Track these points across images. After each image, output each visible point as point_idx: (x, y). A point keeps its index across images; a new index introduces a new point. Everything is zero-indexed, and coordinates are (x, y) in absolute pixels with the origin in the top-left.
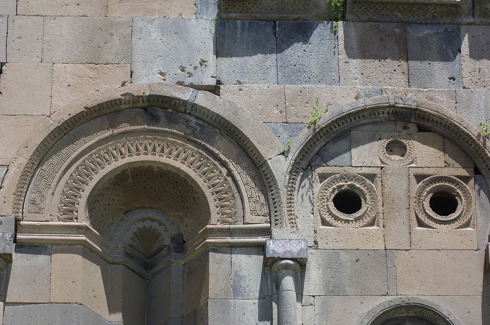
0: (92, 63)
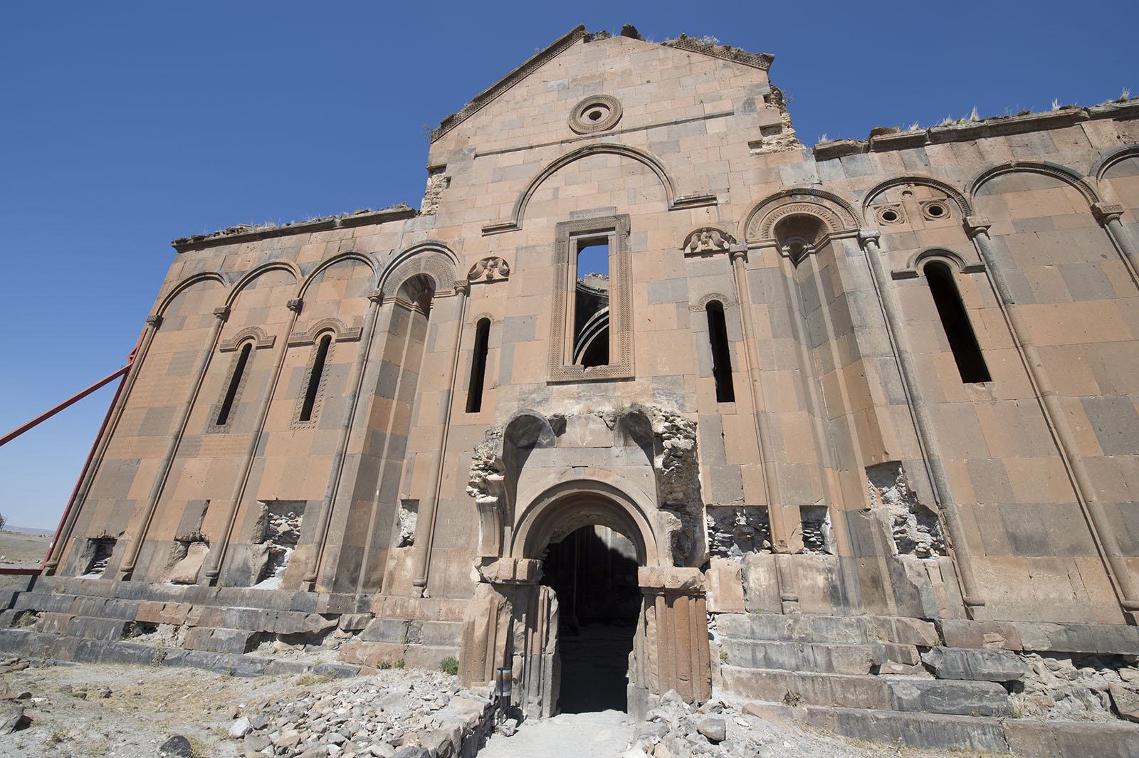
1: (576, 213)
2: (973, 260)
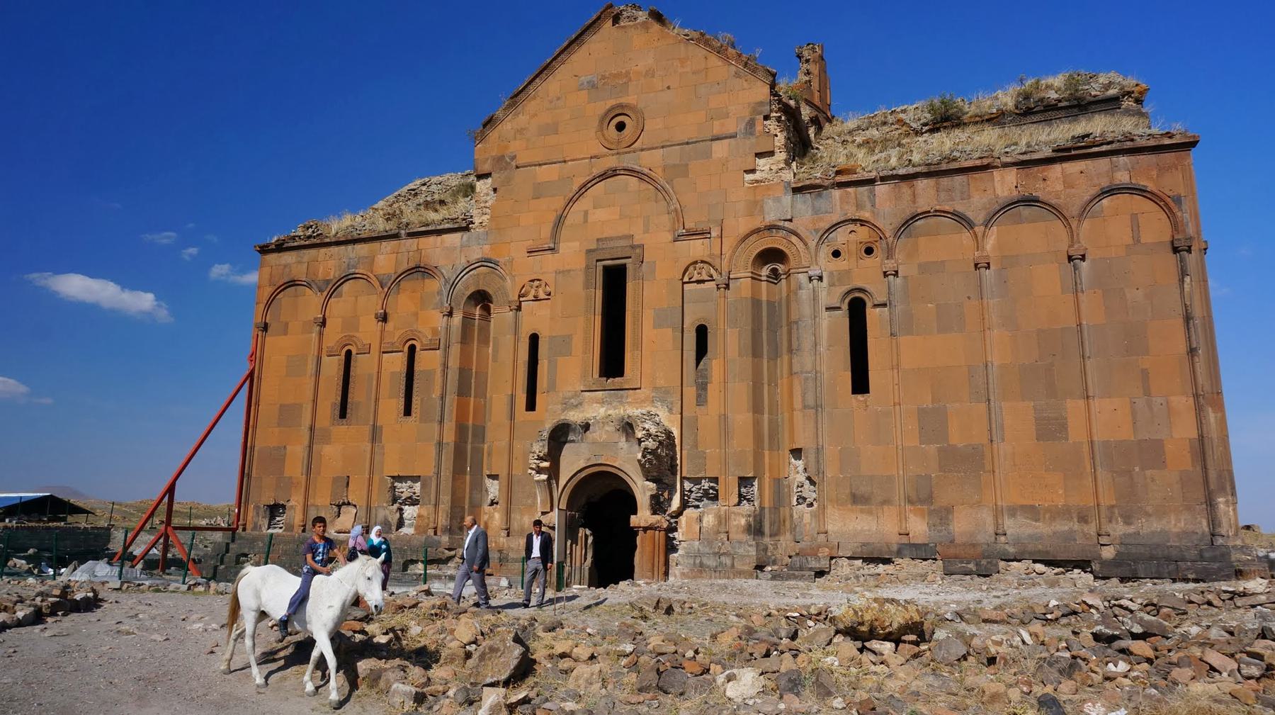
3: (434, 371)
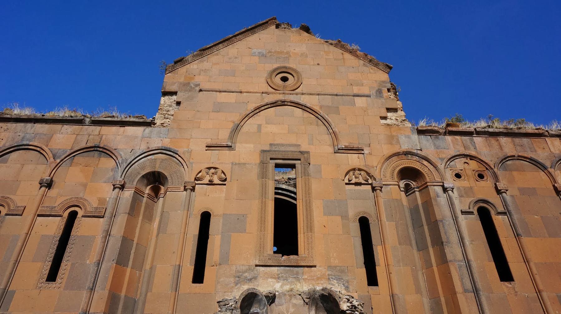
0: (391, 144)
1: (275, 145)
2: (501, 209)
3: (94, 237)
